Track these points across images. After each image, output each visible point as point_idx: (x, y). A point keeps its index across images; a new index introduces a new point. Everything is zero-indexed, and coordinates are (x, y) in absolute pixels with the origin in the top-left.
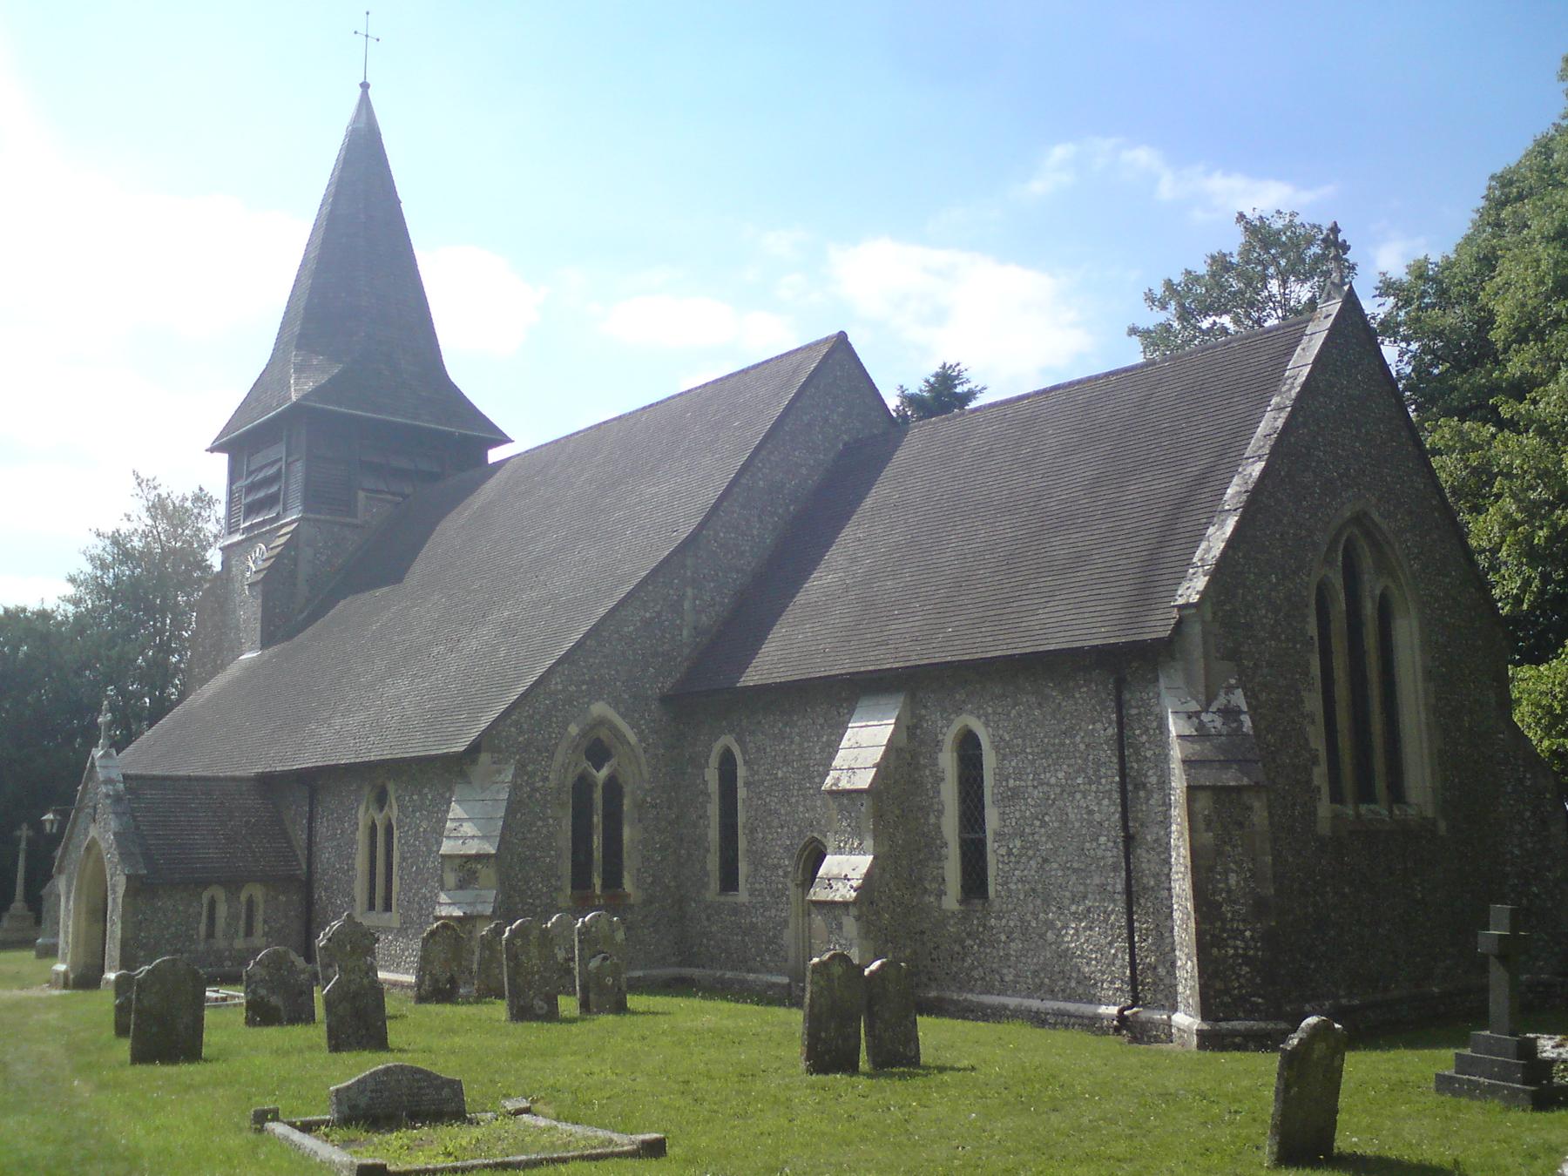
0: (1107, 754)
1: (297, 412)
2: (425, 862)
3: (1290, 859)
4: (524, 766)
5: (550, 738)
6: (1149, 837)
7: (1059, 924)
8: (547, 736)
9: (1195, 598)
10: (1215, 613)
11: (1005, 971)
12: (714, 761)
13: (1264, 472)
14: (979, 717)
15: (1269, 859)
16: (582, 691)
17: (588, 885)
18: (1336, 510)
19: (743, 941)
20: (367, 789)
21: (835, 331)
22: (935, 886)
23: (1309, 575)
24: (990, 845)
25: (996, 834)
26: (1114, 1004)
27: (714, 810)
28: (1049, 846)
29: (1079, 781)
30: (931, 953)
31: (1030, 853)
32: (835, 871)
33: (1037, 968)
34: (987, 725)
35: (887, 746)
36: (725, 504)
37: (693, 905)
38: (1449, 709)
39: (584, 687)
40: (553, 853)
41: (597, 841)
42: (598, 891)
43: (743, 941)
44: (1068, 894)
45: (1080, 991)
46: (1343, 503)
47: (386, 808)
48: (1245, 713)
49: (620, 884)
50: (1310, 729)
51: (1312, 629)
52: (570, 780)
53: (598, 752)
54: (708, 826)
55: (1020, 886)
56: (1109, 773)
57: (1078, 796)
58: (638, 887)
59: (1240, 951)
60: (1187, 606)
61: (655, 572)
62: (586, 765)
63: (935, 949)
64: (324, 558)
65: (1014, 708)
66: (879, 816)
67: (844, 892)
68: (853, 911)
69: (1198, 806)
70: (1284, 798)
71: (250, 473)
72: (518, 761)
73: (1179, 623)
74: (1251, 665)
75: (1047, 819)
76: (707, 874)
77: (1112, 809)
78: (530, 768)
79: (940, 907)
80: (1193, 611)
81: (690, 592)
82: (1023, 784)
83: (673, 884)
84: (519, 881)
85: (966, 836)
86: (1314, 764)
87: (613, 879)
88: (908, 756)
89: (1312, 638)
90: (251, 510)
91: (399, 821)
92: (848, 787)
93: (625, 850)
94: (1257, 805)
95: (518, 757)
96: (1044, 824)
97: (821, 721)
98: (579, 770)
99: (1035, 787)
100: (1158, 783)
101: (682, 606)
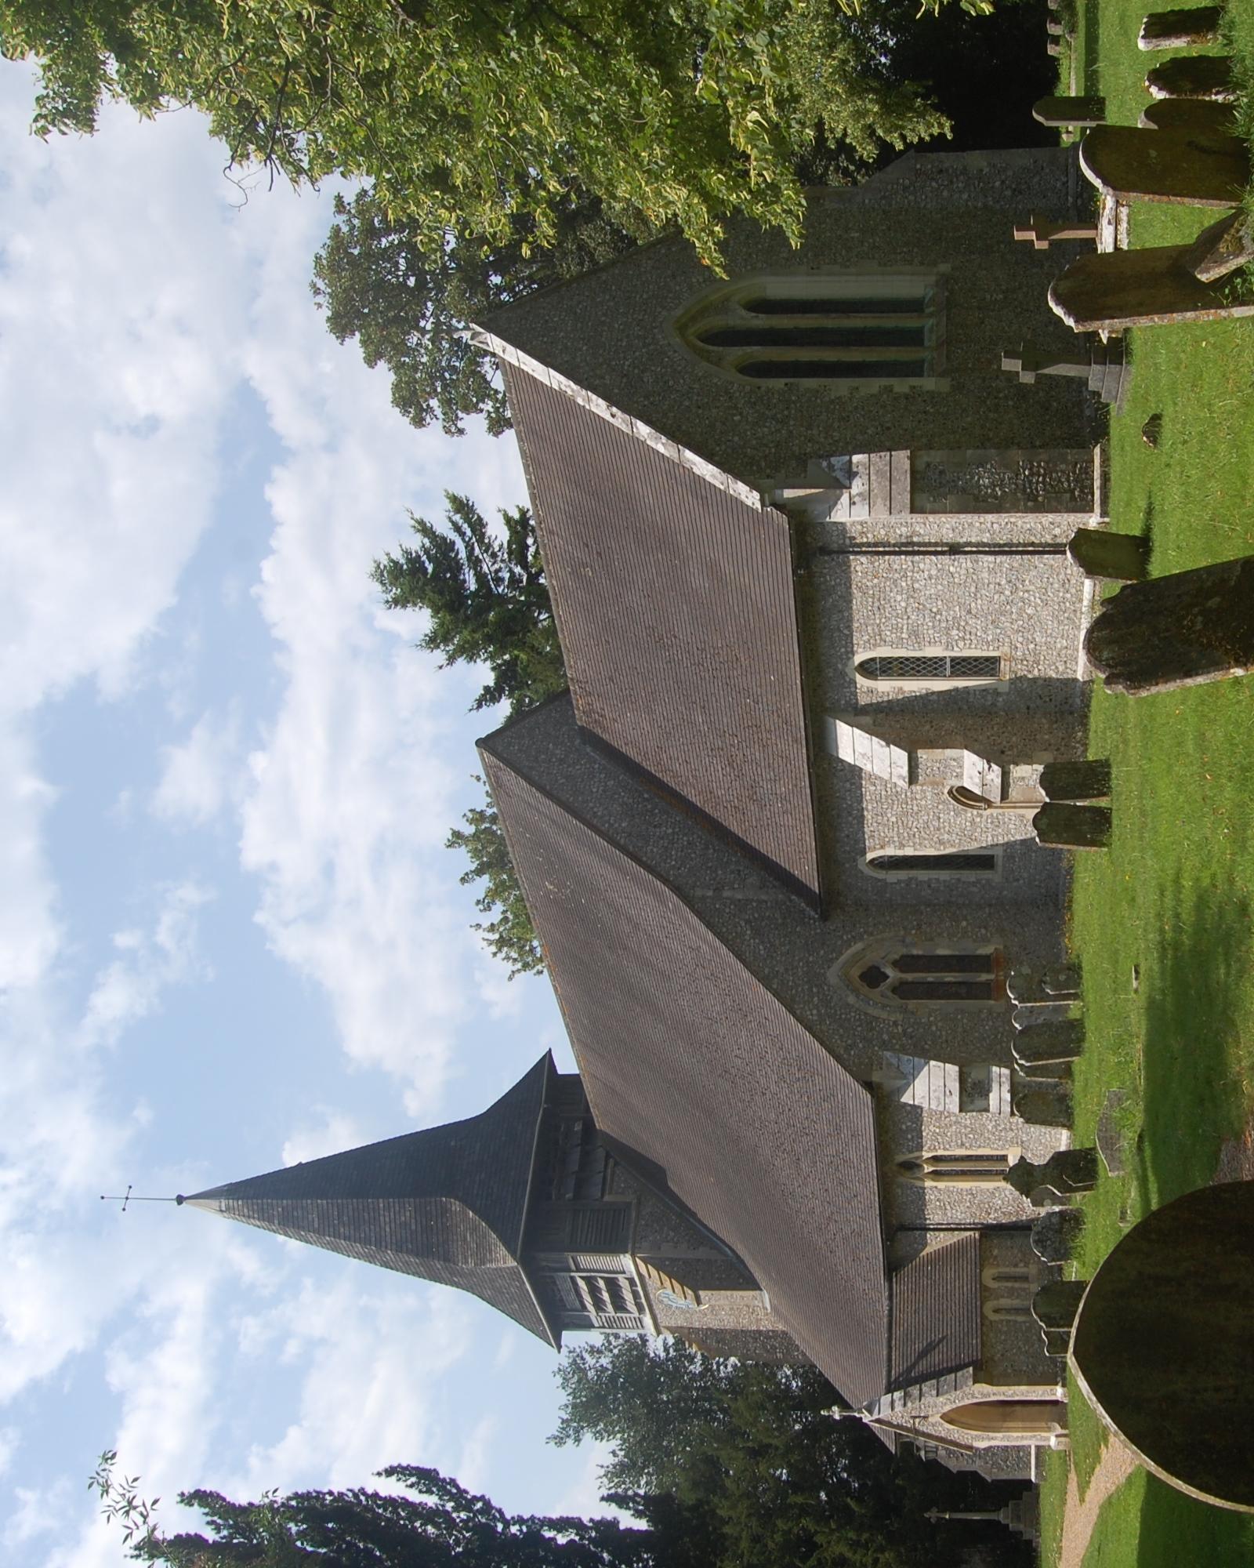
0: (882, 562)
2: (966, 1127)
4: (884, 1042)
7: (1021, 604)
11: (1059, 646)
12: (881, 875)
14: (849, 659)
15: (969, 452)
17: (987, 984)
20: (901, 1180)
21: (475, 748)
22: (989, 698)
24: (957, 653)
25: (947, 649)
27: (923, 875)
28: (957, 608)
29: (904, 584)
31: (963, 623)
32: (977, 780)
33: (1056, 622)
35: (871, 734)
37: (1005, 893)
38: (844, 252)
39: (815, 990)
41: (949, 977)
42: (992, 977)
44: (996, 597)
45: (1073, 591)
47: (918, 1162)
48: (850, 461)
49: (988, 957)
52: (897, 1001)
53: (873, 977)
54: (937, 880)
57: (916, 586)
58: (989, 941)
61: (709, 925)
66: (931, 745)
67: (995, 775)
76: (978, 881)
77: (927, 561)
78: (885, 1037)
79: (1008, 694)
81: (726, 894)
82: (905, 627)
83: (987, 910)
85: (948, 673)
86: (891, 391)
87: (984, 963)
88: (880, 716)
92: (906, 768)
93: (957, 953)
94: (926, 459)
96: (939, 612)
97: (848, 785)
99: (908, 618)
101: (739, 900)
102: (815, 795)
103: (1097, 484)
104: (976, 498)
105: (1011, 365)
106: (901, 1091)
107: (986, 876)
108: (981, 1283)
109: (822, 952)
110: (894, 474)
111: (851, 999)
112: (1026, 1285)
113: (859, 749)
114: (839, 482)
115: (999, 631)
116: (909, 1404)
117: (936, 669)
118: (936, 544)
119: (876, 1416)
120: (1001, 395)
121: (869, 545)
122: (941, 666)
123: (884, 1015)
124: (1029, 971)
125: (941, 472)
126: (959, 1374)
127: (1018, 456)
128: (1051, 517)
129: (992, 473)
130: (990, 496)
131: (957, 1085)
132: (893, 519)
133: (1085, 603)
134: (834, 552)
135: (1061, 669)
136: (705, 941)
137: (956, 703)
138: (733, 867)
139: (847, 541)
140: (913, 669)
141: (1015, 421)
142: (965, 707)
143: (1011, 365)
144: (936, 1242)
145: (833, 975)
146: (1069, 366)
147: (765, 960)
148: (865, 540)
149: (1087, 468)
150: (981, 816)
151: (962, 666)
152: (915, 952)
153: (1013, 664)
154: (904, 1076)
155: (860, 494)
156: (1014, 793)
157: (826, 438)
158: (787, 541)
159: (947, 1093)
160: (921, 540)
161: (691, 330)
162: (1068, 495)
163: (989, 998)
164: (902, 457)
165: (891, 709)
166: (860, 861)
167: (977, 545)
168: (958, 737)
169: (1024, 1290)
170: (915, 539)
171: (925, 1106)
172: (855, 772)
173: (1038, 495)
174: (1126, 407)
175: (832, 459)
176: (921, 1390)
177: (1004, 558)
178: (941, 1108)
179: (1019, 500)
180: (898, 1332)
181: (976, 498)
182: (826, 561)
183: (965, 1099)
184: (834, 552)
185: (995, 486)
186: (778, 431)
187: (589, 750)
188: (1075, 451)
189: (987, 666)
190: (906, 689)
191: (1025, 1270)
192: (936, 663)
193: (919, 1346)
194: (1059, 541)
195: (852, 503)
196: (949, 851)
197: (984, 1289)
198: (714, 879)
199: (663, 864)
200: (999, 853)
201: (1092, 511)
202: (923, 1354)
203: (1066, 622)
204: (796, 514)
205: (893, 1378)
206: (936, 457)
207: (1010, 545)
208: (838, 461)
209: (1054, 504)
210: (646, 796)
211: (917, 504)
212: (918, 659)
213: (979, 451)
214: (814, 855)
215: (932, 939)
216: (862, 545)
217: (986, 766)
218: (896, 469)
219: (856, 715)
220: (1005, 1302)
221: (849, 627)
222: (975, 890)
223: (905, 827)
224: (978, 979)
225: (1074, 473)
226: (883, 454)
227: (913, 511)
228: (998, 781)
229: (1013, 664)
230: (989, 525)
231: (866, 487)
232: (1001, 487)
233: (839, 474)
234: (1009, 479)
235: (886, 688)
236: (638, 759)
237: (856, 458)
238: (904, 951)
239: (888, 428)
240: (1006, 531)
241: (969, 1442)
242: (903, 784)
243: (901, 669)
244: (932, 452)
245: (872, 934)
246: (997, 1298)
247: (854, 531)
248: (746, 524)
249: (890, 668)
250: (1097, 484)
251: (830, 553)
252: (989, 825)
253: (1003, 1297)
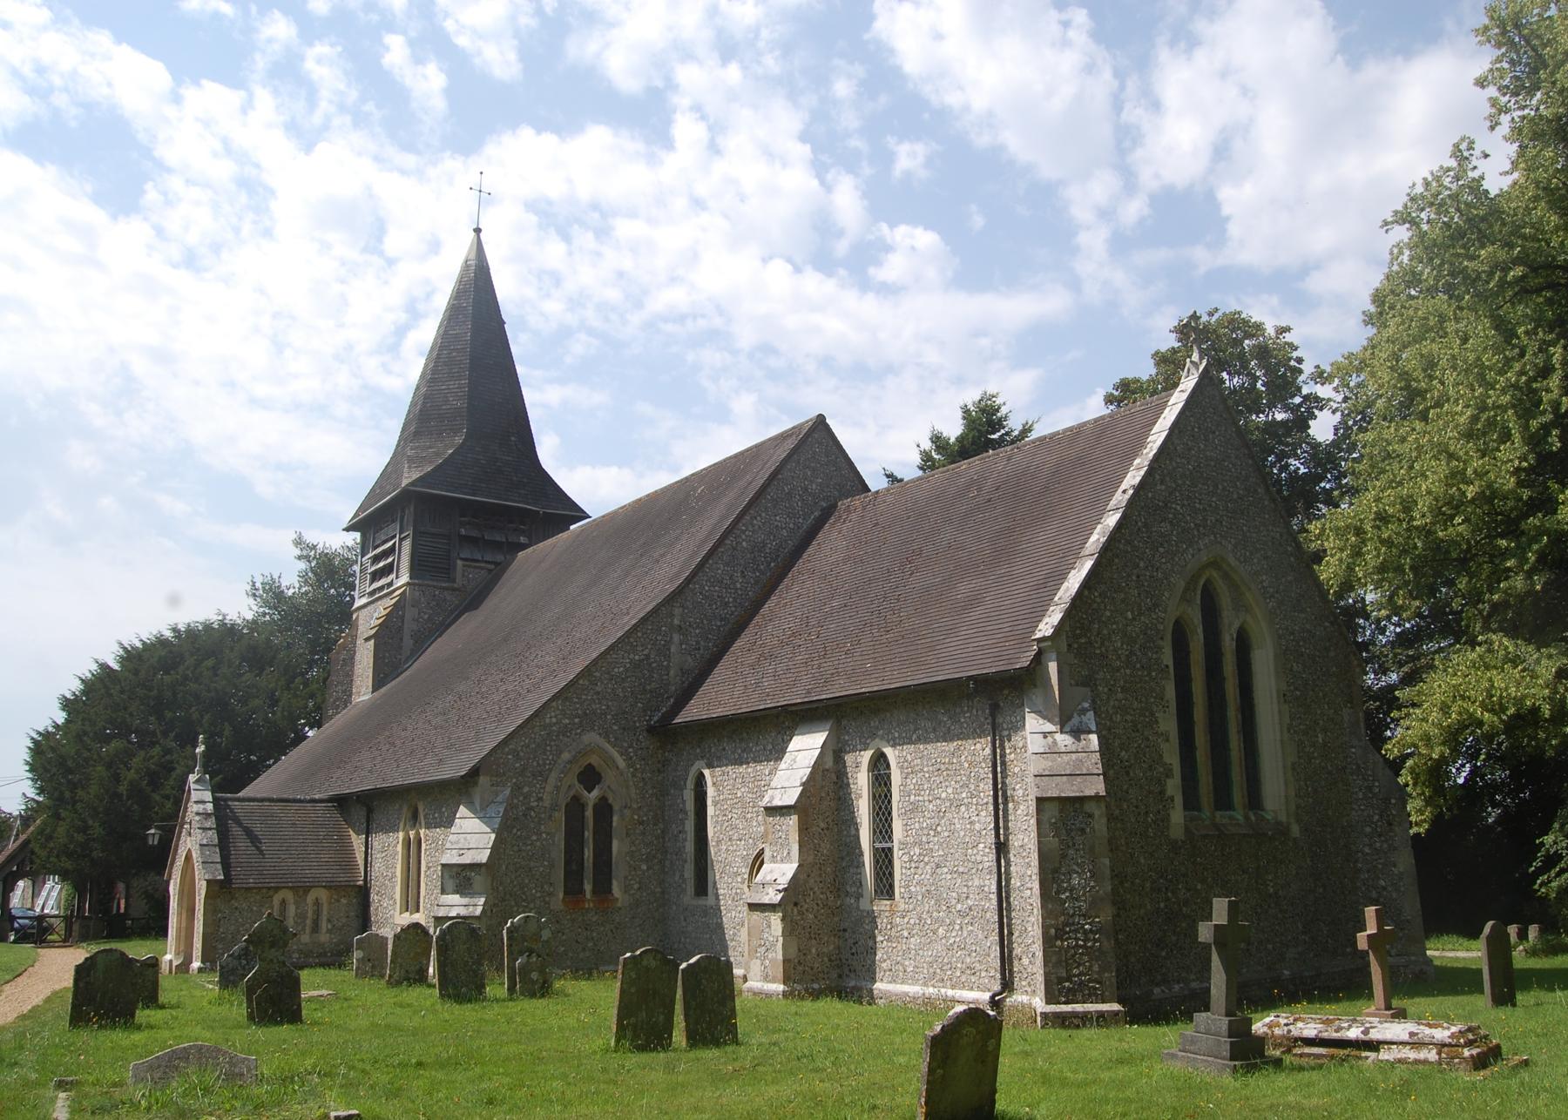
0: (985, 771)
1: (406, 496)
3: (1143, 861)
5: (545, 764)
6: (1016, 844)
8: (541, 762)
9: (1049, 632)
10: (1069, 646)
11: (907, 963)
12: (690, 784)
13: (1120, 525)
15: (1107, 861)
16: (575, 724)
17: (582, 891)
18: (1193, 556)
19: (711, 938)
20: (405, 809)
23: (1165, 612)
24: (897, 853)
25: (900, 842)
26: (989, 990)
28: (941, 853)
29: (964, 795)
30: (851, 948)
31: (926, 859)
32: (768, 878)
33: (930, 959)
36: (711, 562)
37: (674, 908)
39: (577, 720)
40: (546, 863)
41: (588, 853)
42: (588, 895)
43: (711, 938)
44: (954, 894)
46: (1200, 550)
48: (1090, 732)
49: (610, 891)
50: (1164, 746)
51: (1167, 658)
53: (590, 777)
54: (685, 840)
55: (918, 888)
56: (986, 787)
57: (963, 808)
58: (626, 892)
59: (1081, 943)
60: (1044, 639)
61: (644, 620)
62: (579, 788)
63: (854, 944)
64: (426, 616)
65: (915, 730)
66: (804, 829)
67: (773, 897)
69: (1045, 818)
70: (1137, 807)
71: (375, 548)
72: (515, 783)
73: (1040, 653)
74: (1106, 690)
75: (939, 829)
76: (684, 881)
78: (526, 789)
79: (858, 908)
80: (1050, 643)
81: (676, 637)
82: (921, 798)
83: (658, 890)
84: (515, 886)
85: (878, 845)
86: (1167, 776)
88: (834, 777)
89: (1167, 666)
90: (376, 576)
92: (780, 804)
93: (614, 860)
94: (1097, 813)
95: (514, 780)
96: (937, 834)
97: (770, 747)
98: (572, 793)
99: (930, 802)
100: (1023, 796)
101: (669, 649)
102: (758, 714)
103: (1078, 1007)
104: (1056, 871)
105: (1220, 910)
106: (470, 806)
107: (688, 887)
108: (312, 887)
109: (616, 728)
110: (1079, 779)
111: (566, 756)
112: (307, 931)
113: (800, 755)
114: (1066, 719)
115: (920, 898)
116: (197, 818)
117: (881, 832)
118: (1006, 828)
119: (193, 786)
120: (1169, 894)
121: (1003, 756)
122: (884, 837)
123: (549, 788)
124: (544, 938)
125: (1083, 831)
126: (219, 866)
127: (1105, 916)
128: (1040, 954)
129: (1084, 888)
130: (1059, 885)
131: (468, 862)
132: (1030, 779)
133: (950, 993)
134: (994, 720)
135: (884, 965)
136: (630, 619)
137: (848, 854)
138: (702, 643)
139: (1006, 733)
140: (880, 808)
141: (1142, 911)
142: (844, 864)
143: (1220, 910)
144: (357, 841)
145: (591, 738)
146: (1224, 987)
147: (608, 673)
148: (1008, 751)
149: (1097, 995)
150: (743, 883)
151: (884, 859)
152: (615, 818)
153: (887, 914)
154: (483, 808)
155: (1055, 742)
156: (757, 916)
157: (1114, 707)
158: (1002, 668)
159: (461, 851)
160: (1010, 811)
162: (1064, 975)
163: (566, 893)
164: (1097, 787)
165: (841, 787)
166: (699, 764)
167: (1008, 873)
168: (812, 857)
170: (1011, 805)
171: (453, 829)
172: (778, 753)
173: (1062, 941)
174: (1177, 1067)
175: (1092, 712)
176: (210, 829)
177: (995, 902)
178: (448, 845)
179: (1057, 919)
180: (276, 807)
181: (1056, 871)
182: (984, 711)
183: (455, 869)
184: (994, 720)
185: (1071, 891)
186: (1119, 658)
187: (816, 514)
188: (1114, 980)
189: (885, 886)
190: (860, 800)
191: (324, 930)
192: (887, 832)
193: (258, 829)
194: (1016, 963)
195: (1045, 735)
196: (712, 850)
197: (307, 890)
198: (690, 626)
199: (705, 578)
200: (711, 901)
201: (1048, 1003)
202: (249, 833)
203: (931, 970)
204: (1035, 670)
205: (230, 803)
206: (1100, 824)
207: (1009, 909)
208: (1090, 719)
209: (1054, 959)
210: (772, 564)
211: (1047, 805)
212: (890, 813)
213: (1108, 872)
214: (704, 717)
215: (628, 835)
216: (1003, 749)
217: (781, 887)
218: (1085, 781)
219: (834, 751)
220: (292, 910)
221: (919, 741)
222: (677, 879)
223: (733, 806)
224: (586, 882)
225: (1090, 981)
226: (1100, 766)
227: (1040, 800)
228: (766, 900)
229: (887, 914)
230: (1029, 885)
231: (1063, 749)
232: (1071, 898)
233: (1075, 720)
234: (1079, 907)
235: (861, 781)
236: (805, 556)
237: (1094, 738)
238: (616, 808)
239: (1128, 773)
240: (1023, 905)
241: (174, 877)
242: (765, 802)
243: (880, 796)
244: (1104, 820)
245: (634, 776)
246: (296, 903)
247: (1017, 739)
248: (1020, 627)
249: (880, 785)
250: (1078, 1007)
251: (993, 716)
252: (734, 891)
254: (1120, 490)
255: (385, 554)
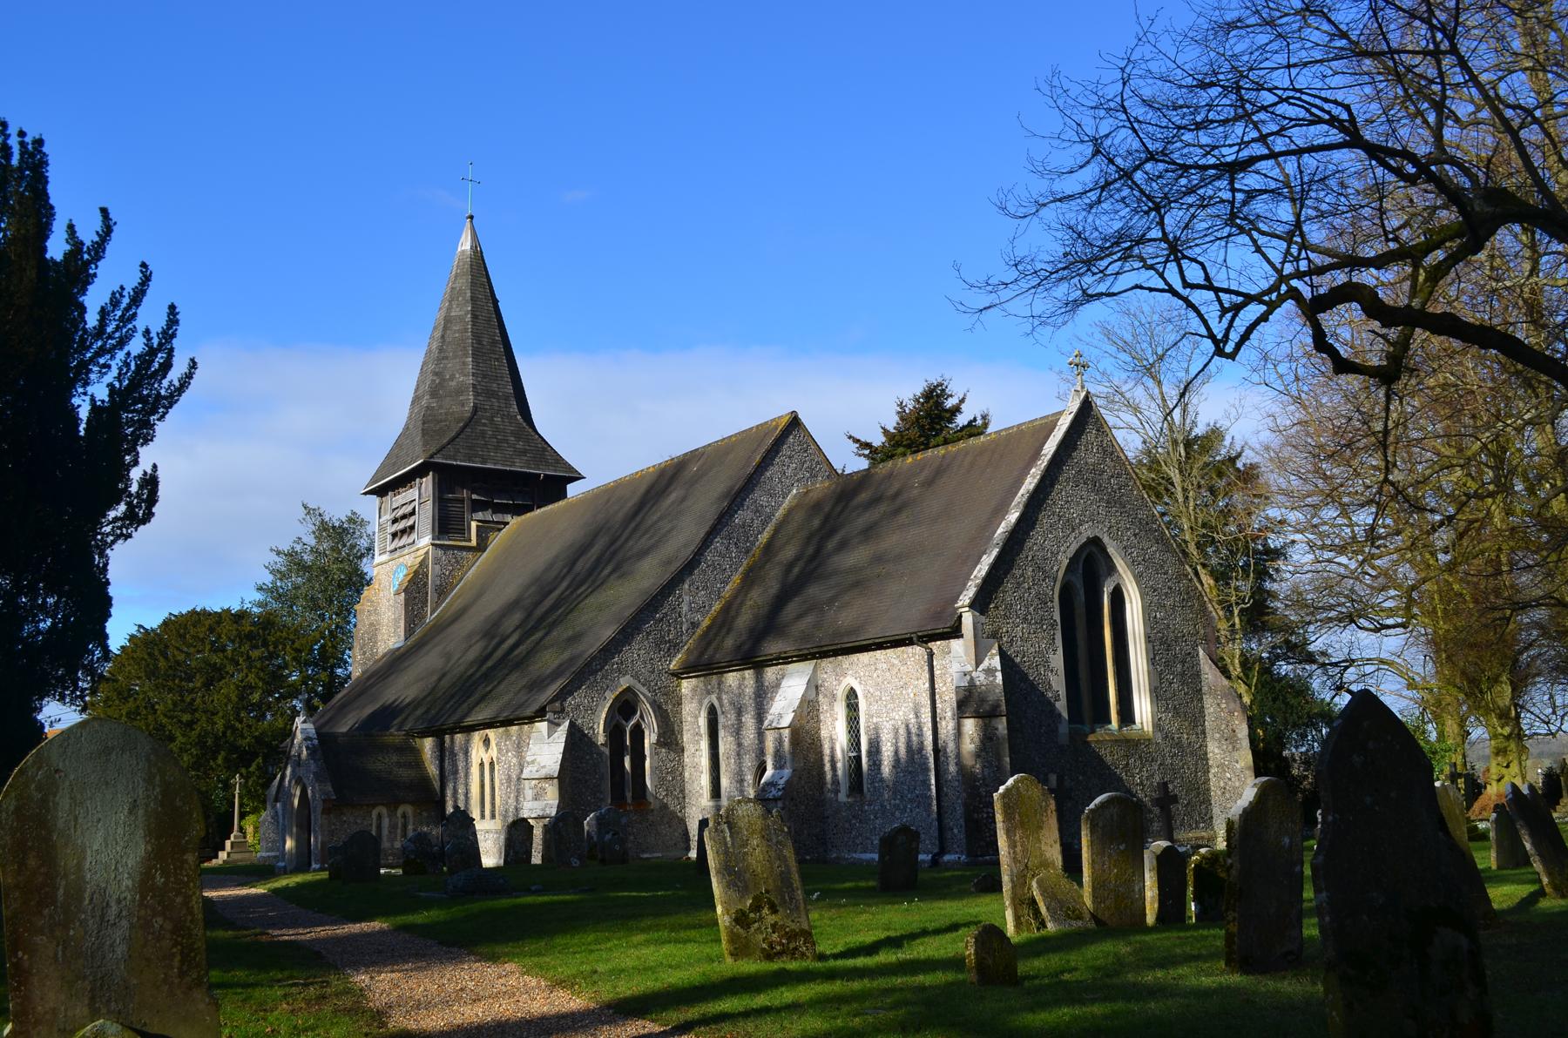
3: (1037, 759)
17: (624, 797)
34: (860, 683)
42: (629, 801)
68: (780, 804)
79: (837, 800)
91: (498, 759)
161: (1094, 549)
169: (396, 836)
212: (858, 731)
217: (780, 787)
220: (386, 822)
239: (1026, 698)
246: (389, 816)
253: (390, 821)
254: (1019, 494)
255: (404, 517)
